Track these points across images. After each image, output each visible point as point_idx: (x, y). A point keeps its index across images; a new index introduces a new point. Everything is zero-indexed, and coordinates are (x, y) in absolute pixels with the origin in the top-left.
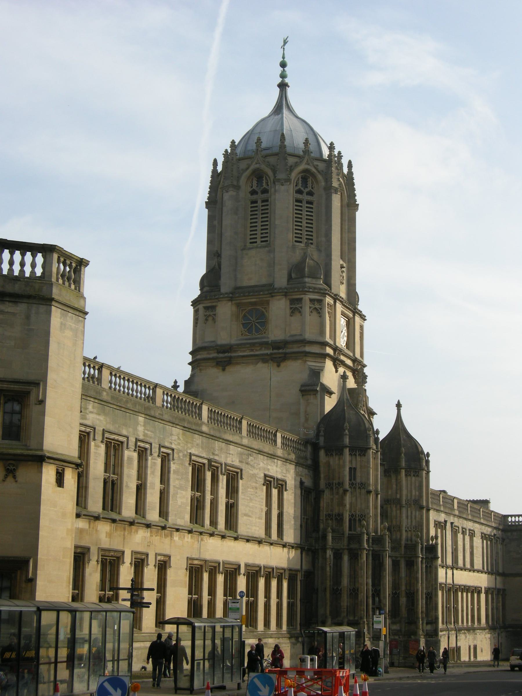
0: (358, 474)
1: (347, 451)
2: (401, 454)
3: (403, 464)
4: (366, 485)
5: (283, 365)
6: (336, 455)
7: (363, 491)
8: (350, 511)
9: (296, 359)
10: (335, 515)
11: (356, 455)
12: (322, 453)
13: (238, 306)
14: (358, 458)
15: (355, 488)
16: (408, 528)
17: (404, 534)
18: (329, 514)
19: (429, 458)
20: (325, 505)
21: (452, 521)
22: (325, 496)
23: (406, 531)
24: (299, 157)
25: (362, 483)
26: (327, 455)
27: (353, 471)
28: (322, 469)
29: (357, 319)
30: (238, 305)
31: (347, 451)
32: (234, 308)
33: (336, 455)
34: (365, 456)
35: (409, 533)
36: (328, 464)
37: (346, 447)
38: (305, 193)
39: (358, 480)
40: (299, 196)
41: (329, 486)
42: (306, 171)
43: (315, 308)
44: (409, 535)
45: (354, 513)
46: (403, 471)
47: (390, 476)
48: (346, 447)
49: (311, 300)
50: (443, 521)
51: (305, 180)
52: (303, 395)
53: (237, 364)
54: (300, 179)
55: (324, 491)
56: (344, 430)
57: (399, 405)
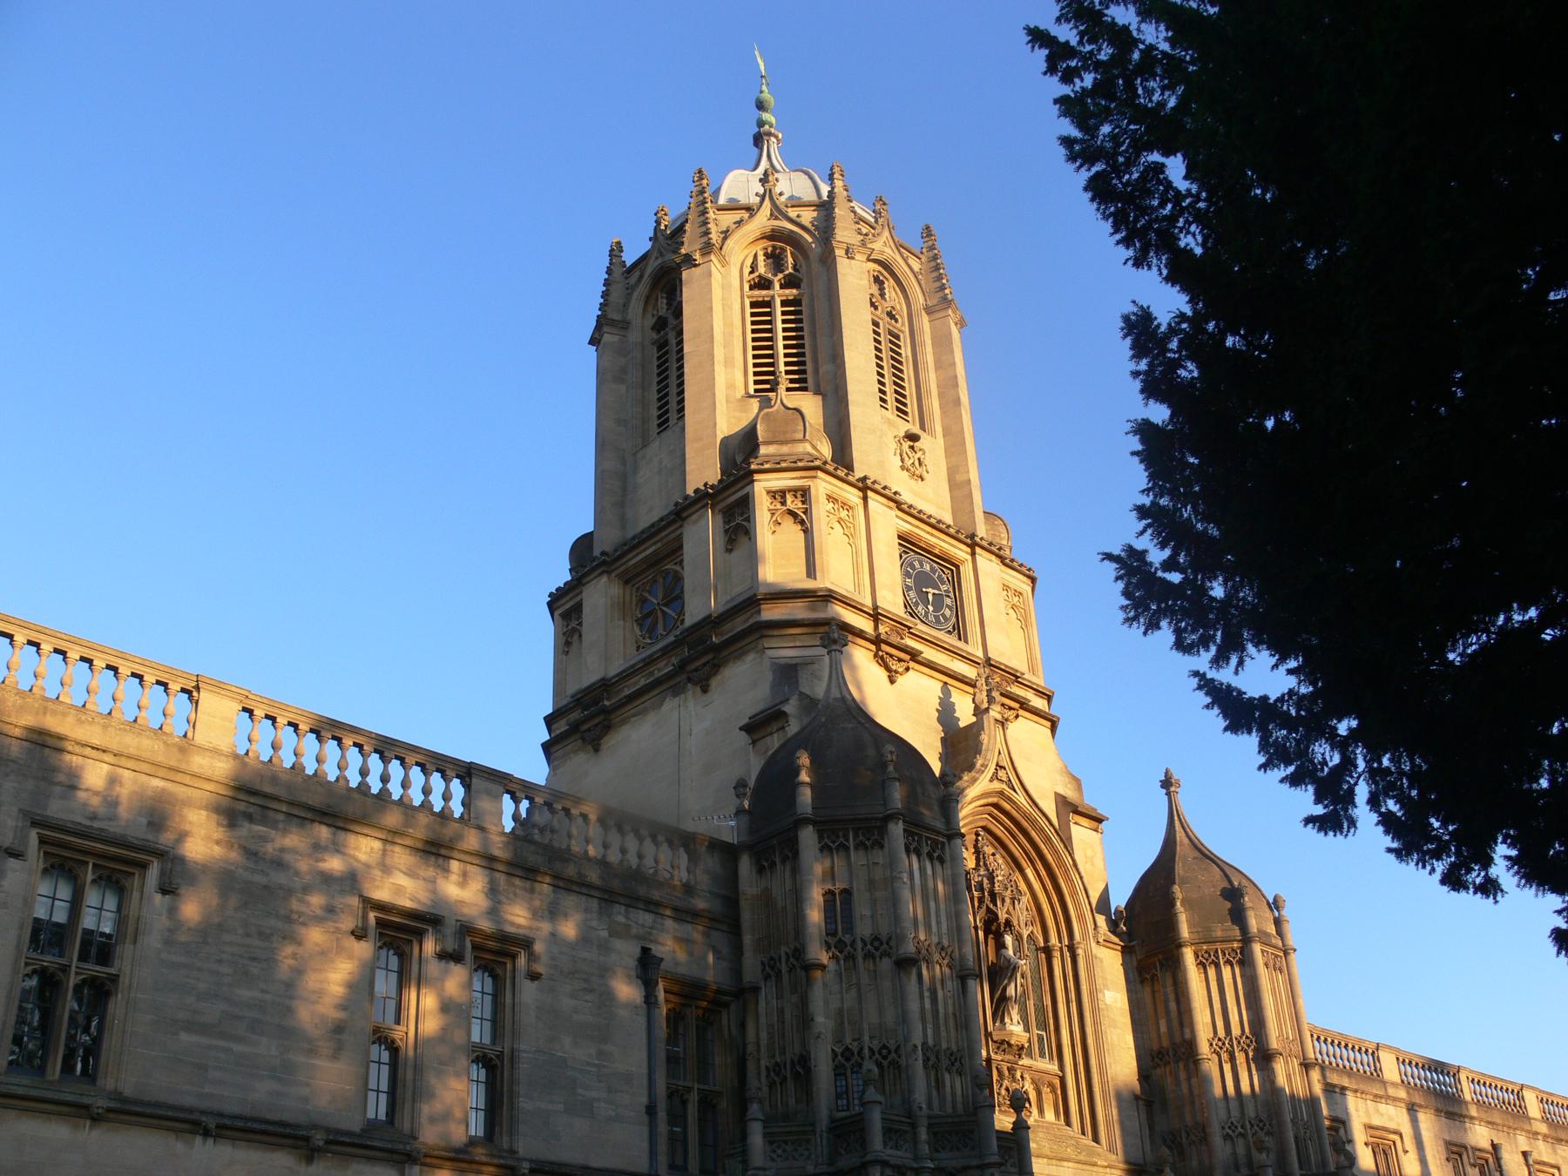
0: (862, 908)
1: (808, 836)
2: (1173, 905)
3: (1185, 932)
4: (892, 943)
5: (714, 682)
6: (783, 862)
7: (886, 964)
8: (839, 1040)
9: (740, 655)
10: (792, 1061)
11: (847, 849)
12: (745, 865)
13: (626, 582)
14: (858, 858)
15: (851, 957)
16: (1232, 1126)
17: (1221, 1149)
18: (777, 1064)
19: (1284, 913)
20: (764, 1035)
21: (1526, 1148)
22: (762, 1004)
23: (1227, 1137)
24: (748, 209)
25: (876, 938)
26: (761, 870)
27: (839, 905)
28: (746, 917)
29: (986, 563)
30: (627, 580)
31: (808, 837)
32: (615, 589)
33: (783, 862)
34: (882, 847)
35: (1241, 1141)
36: (766, 899)
37: (805, 821)
38: (777, 286)
39: (864, 929)
40: (761, 294)
41: (771, 969)
42: (773, 235)
43: (791, 513)
44: (1241, 1150)
45: (855, 1047)
46: (1188, 955)
47: (1154, 978)
48: (805, 821)
49: (773, 494)
50: (1486, 1145)
51: (775, 259)
52: (754, 742)
53: (624, 722)
54: (761, 258)
55: (755, 990)
56: (798, 774)
57: (1167, 783)
